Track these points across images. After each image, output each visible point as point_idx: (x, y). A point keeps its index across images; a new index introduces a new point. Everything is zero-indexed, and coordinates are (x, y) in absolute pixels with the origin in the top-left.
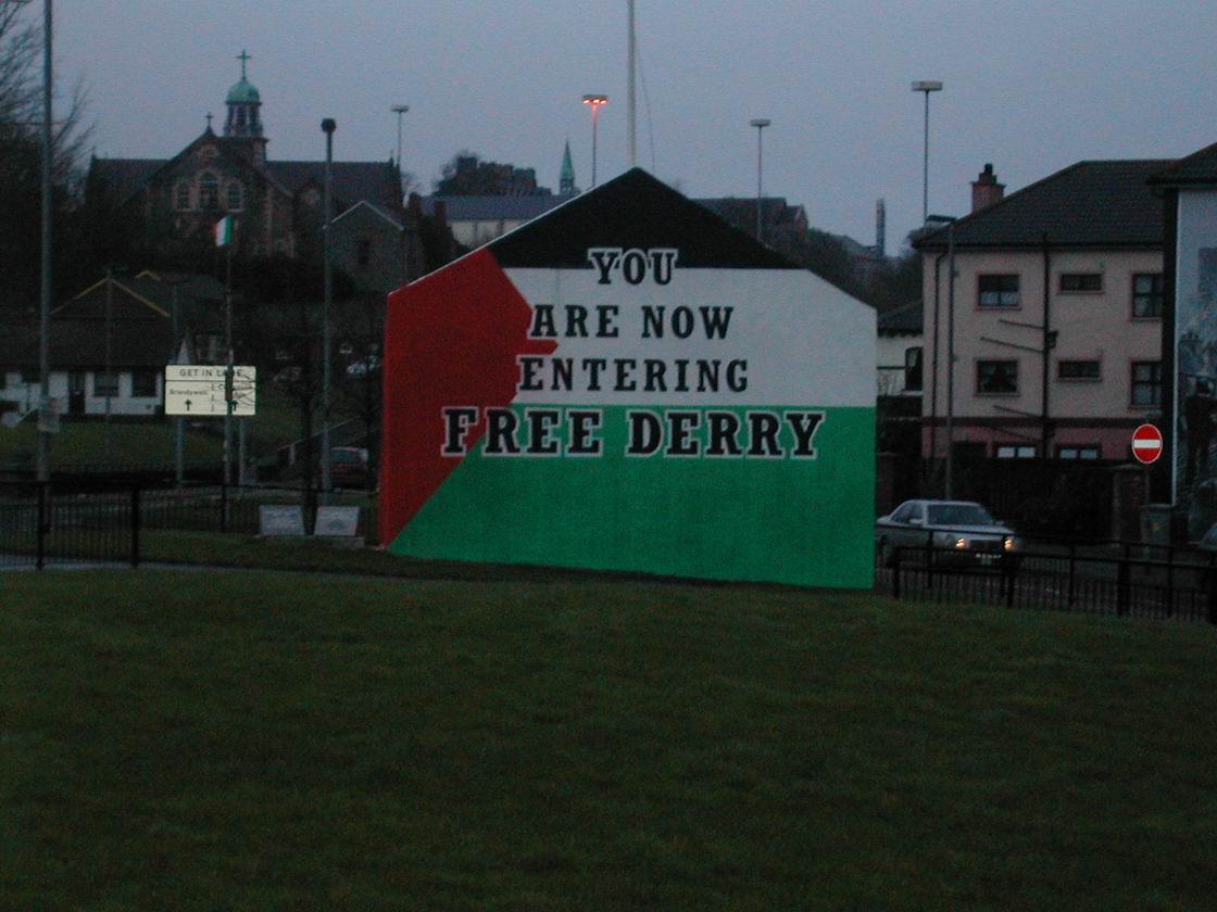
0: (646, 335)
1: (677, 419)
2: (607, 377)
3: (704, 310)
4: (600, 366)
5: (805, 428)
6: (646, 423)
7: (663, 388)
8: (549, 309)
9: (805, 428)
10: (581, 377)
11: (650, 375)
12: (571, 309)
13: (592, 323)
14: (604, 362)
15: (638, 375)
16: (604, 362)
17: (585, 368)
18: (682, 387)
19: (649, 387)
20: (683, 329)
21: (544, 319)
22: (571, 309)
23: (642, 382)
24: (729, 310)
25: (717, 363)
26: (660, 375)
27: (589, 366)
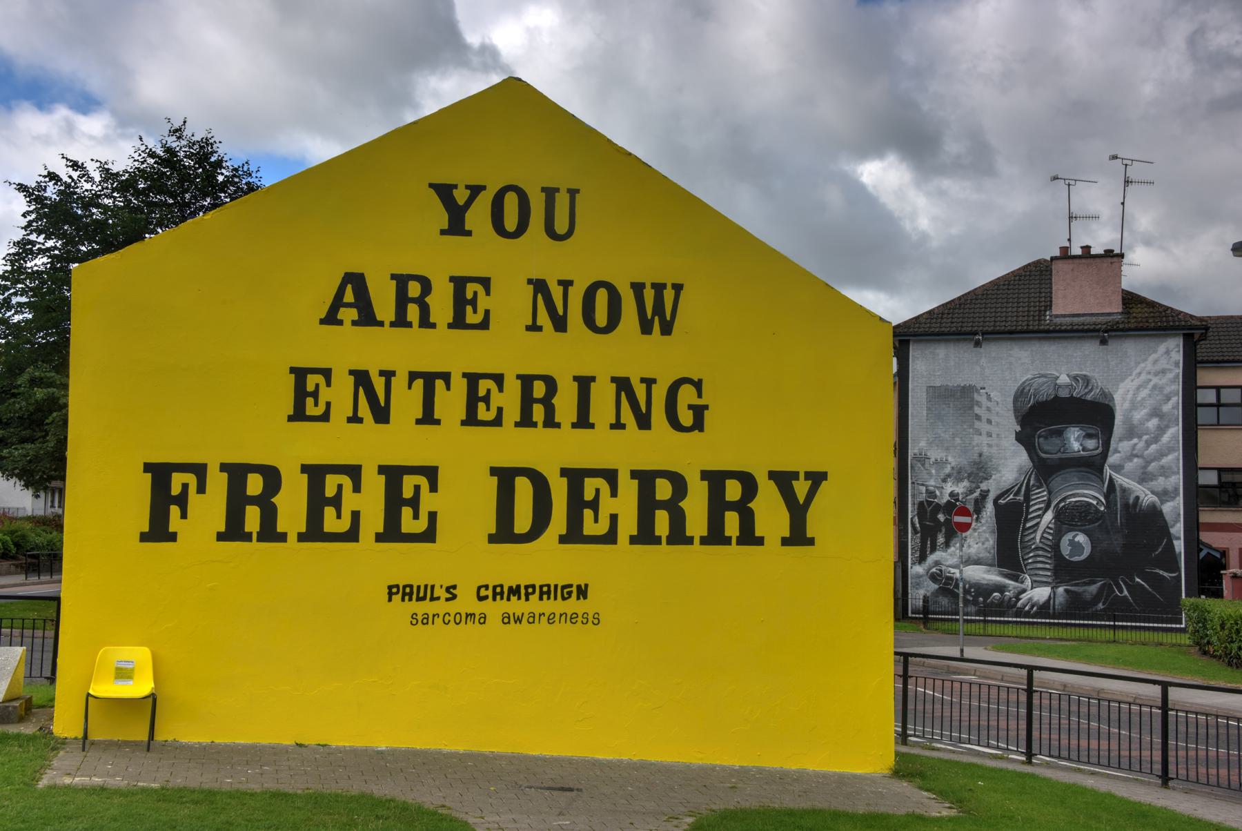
1: (575, 477)
2: (451, 402)
4: (439, 383)
10: (407, 402)
11: (527, 401)
14: (446, 377)
15: (509, 400)
16: (446, 377)
19: (526, 421)
26: (547, 402)
27: (419, 384)
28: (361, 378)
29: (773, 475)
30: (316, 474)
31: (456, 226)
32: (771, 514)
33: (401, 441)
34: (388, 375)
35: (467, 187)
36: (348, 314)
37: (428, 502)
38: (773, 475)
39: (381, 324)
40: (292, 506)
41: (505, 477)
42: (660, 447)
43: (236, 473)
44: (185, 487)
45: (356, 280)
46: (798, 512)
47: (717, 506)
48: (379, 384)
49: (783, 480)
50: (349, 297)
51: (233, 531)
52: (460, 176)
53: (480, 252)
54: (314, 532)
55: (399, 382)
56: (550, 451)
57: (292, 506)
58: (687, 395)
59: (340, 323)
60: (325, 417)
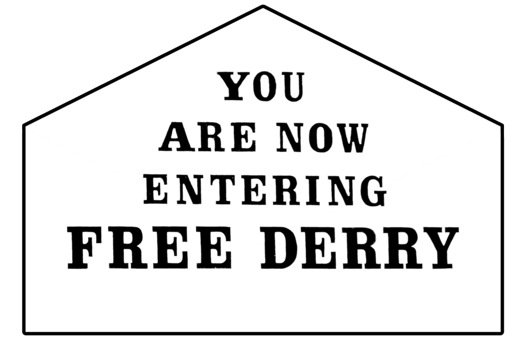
4: (228, 182)
5: (444, 242)
9: (444, 242)
10: (210, 192)
14: (232, 178)
15: (269, 190)
23: (272, 197)
25: (351, 179)
27: (217, 182)
28: (184, 179)
29: (426, 230)
30: (161, 232)
33: (209, 213)
34: (199, 177)
35: (239, 73)
36: (174, 145)
37: (225, 246)
38: (426, 230)
39: (193, 150)
41: (269, 233)
42: (359, 215)
43: (118, 232)
44: (90, 239)
45: (178, 126)
46: (442, 251)
47: (394, 247)
48: (194, 183)
49: (433, 233)
50: (174, 135)
52: (236, 70)
53: (248, 108)
54: (162, 263)
55: (205, 181)
56: (295, 218)
58: (373, 186)
59: (170, 149)
60: (165, 201)
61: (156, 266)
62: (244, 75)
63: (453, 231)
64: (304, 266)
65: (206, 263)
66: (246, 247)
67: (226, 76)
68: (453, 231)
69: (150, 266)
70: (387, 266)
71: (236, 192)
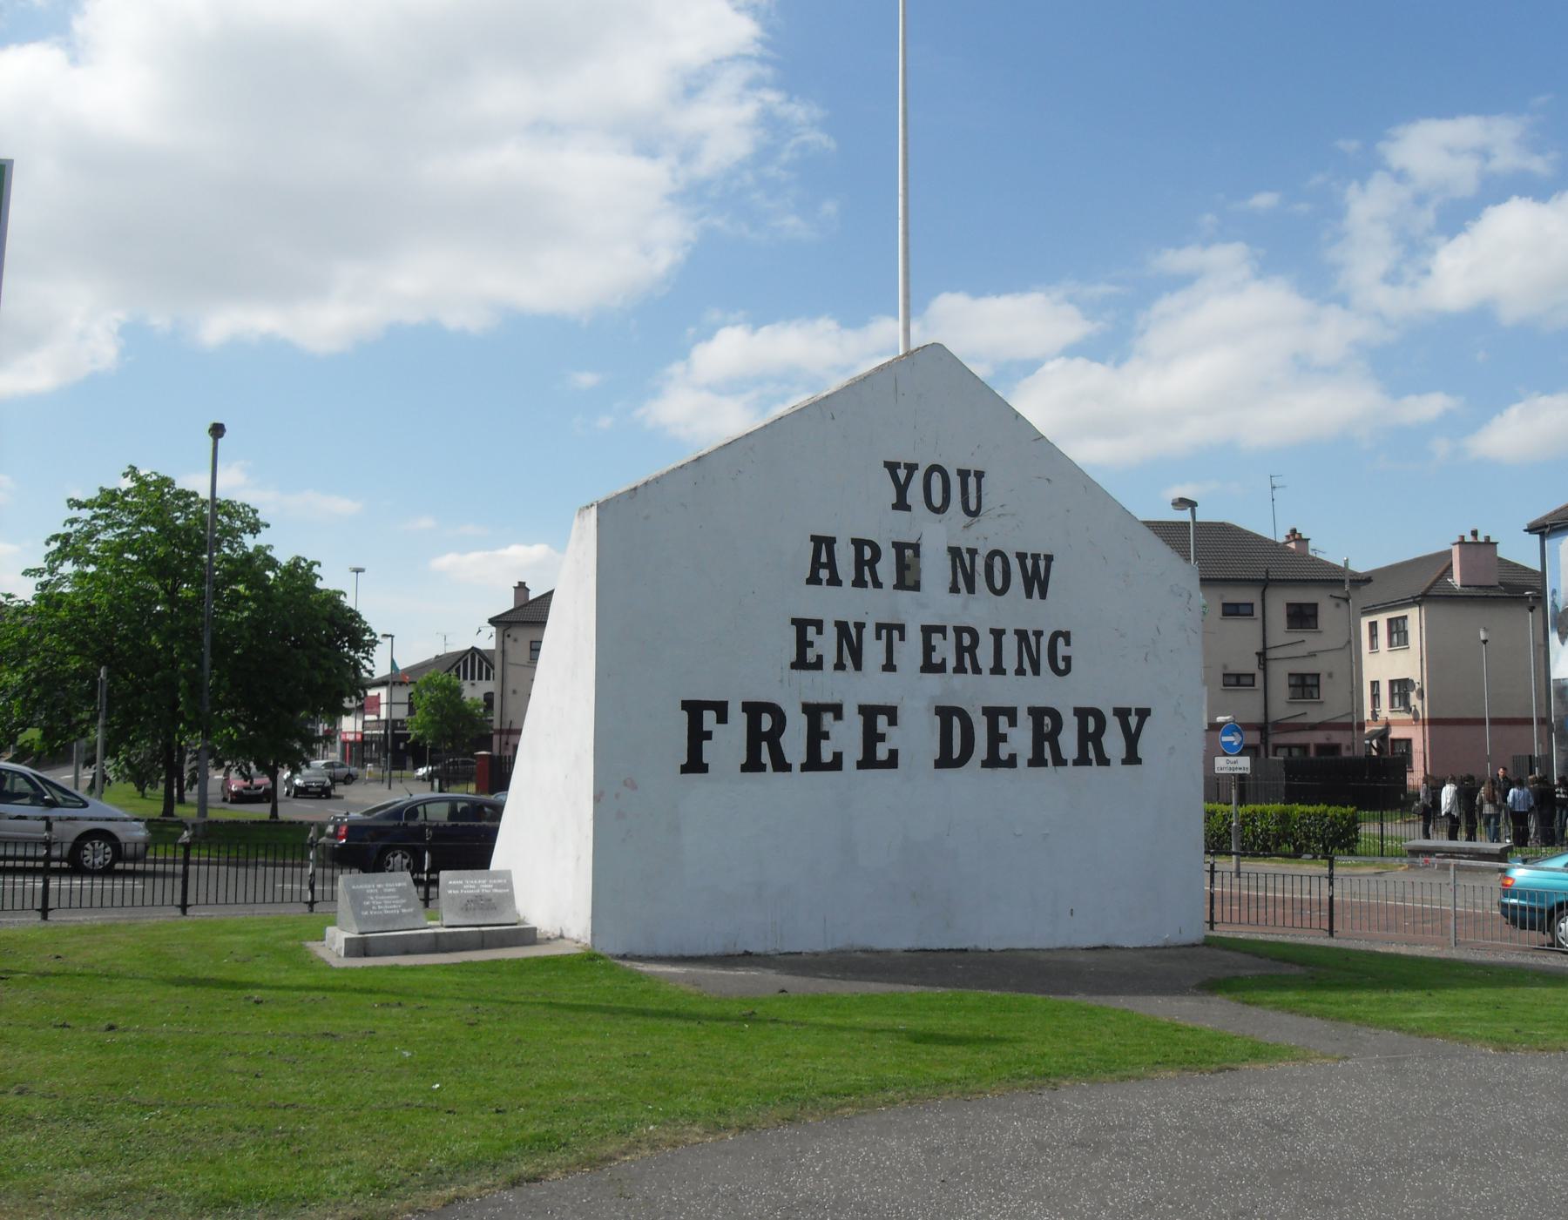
0: (954, 589)
1: (992, 713)
3: (1021, 557)
4: (896, 634)
6: (956, 721)
7: (977, 670)
8: (830, 542)
12: (859, 544)
13: (886, 568)
17: (879, 637)
18: (998, 669)
19: (959, 669)
20: (998, 584)
21: (824, 559)
22: (859, 544)
24: (1049, 559)
25: (1038, 634)
27: (884, 632)
30: (813, 712)
31: (901, 504)
32: (1114, 742)
40: (794, 744)
41: (946, 714)
43: (753, 710)
46: (1132, 739)
49: (1122, 714)
51: (752, 764)
54: (813, 763)
55: (869, 633)
56: (974, 692)
57: (794, 744)
61: (804, 768)
62: (911, 468)
63: (1144, 714)
64: (985, 764)
65: (868, 761)
66: (915, 736)
67: (892, 467)
68: (1144, 714)
69: (796, 767)
70: (1076, 763)
71: (910, 651)
